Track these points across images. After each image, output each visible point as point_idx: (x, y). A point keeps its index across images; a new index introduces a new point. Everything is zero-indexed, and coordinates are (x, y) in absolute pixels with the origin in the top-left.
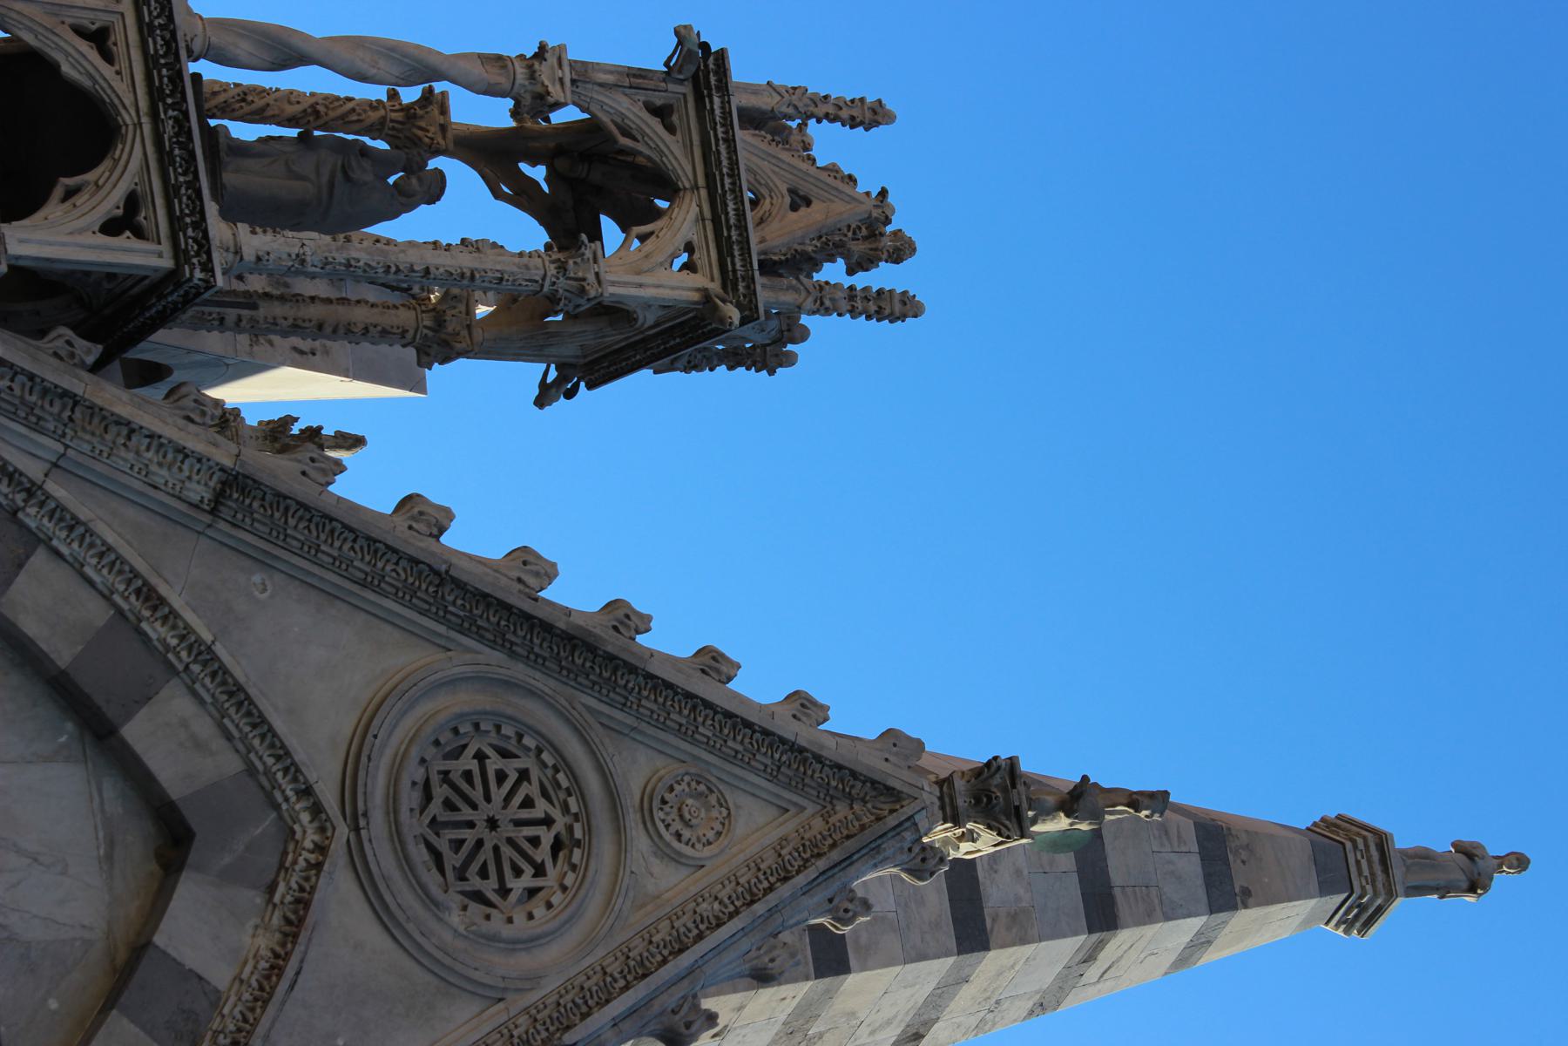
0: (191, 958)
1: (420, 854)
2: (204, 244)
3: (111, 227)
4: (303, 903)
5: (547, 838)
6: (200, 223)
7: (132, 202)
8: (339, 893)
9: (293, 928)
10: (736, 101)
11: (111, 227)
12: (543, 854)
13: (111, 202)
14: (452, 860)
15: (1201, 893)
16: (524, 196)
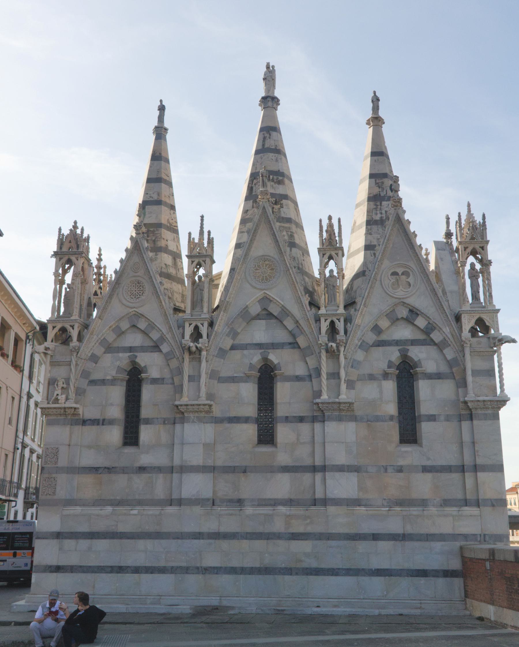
0: (145, 326)
1: (138, 300)
2: (75, 320)
3: (73, 329)
4: (141, 314)
5: (137, 284)
6: (72, 320)
7: (71, 326)
8: (140, 310)
9: (143, 316)
10: (59, 251)
11: (73, 329)
12: (139, 285)
13: (71, 329)
14: (138, 296)
15: (159, 162)
16: (69, 268)
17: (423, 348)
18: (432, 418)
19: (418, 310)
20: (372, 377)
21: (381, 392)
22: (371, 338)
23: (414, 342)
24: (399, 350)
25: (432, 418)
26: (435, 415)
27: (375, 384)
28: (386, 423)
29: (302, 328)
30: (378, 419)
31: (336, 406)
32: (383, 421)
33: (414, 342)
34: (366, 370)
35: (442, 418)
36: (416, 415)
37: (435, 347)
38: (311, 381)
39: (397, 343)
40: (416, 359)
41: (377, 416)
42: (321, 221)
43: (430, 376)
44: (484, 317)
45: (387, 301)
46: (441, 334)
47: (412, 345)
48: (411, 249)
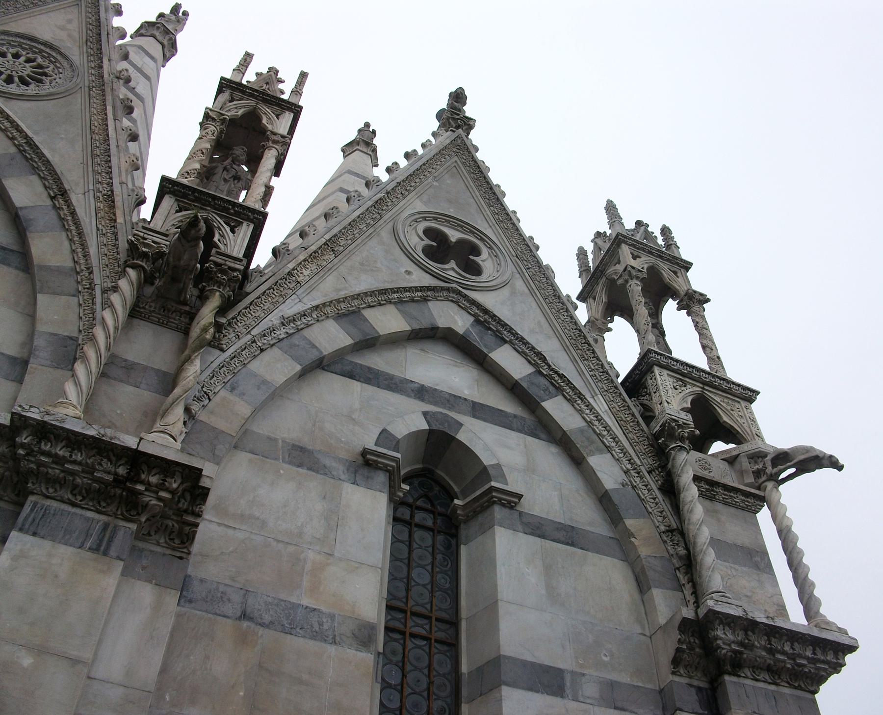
17: (514, 438)
18: (549, 680)
19: (505, 325)
20: (302, 457)
21: (334, 519)
22: (331, 337)
23: (478, 410)
24: (425, 414)
25: (549, 680)
26: (560, 672)
27: (314, 484)
28: (332, 650)
29: (73, 213)
30: (295, 621)
31: (106, 470)
32: (318, 635)
33: (478, 410)
34: (287, 423)
35: (590, 690)
36: (464, 668)
37: (554, 449)
38: (20, 381)
39: (421, 393)
40: (487, 460)
41: (295, 606)
42: (248, 58)
43: (538, 528)
44: (716, 398)
45: (409, 273)
46: (580, 412)
47: (474, 416)
48: (489, 206)
